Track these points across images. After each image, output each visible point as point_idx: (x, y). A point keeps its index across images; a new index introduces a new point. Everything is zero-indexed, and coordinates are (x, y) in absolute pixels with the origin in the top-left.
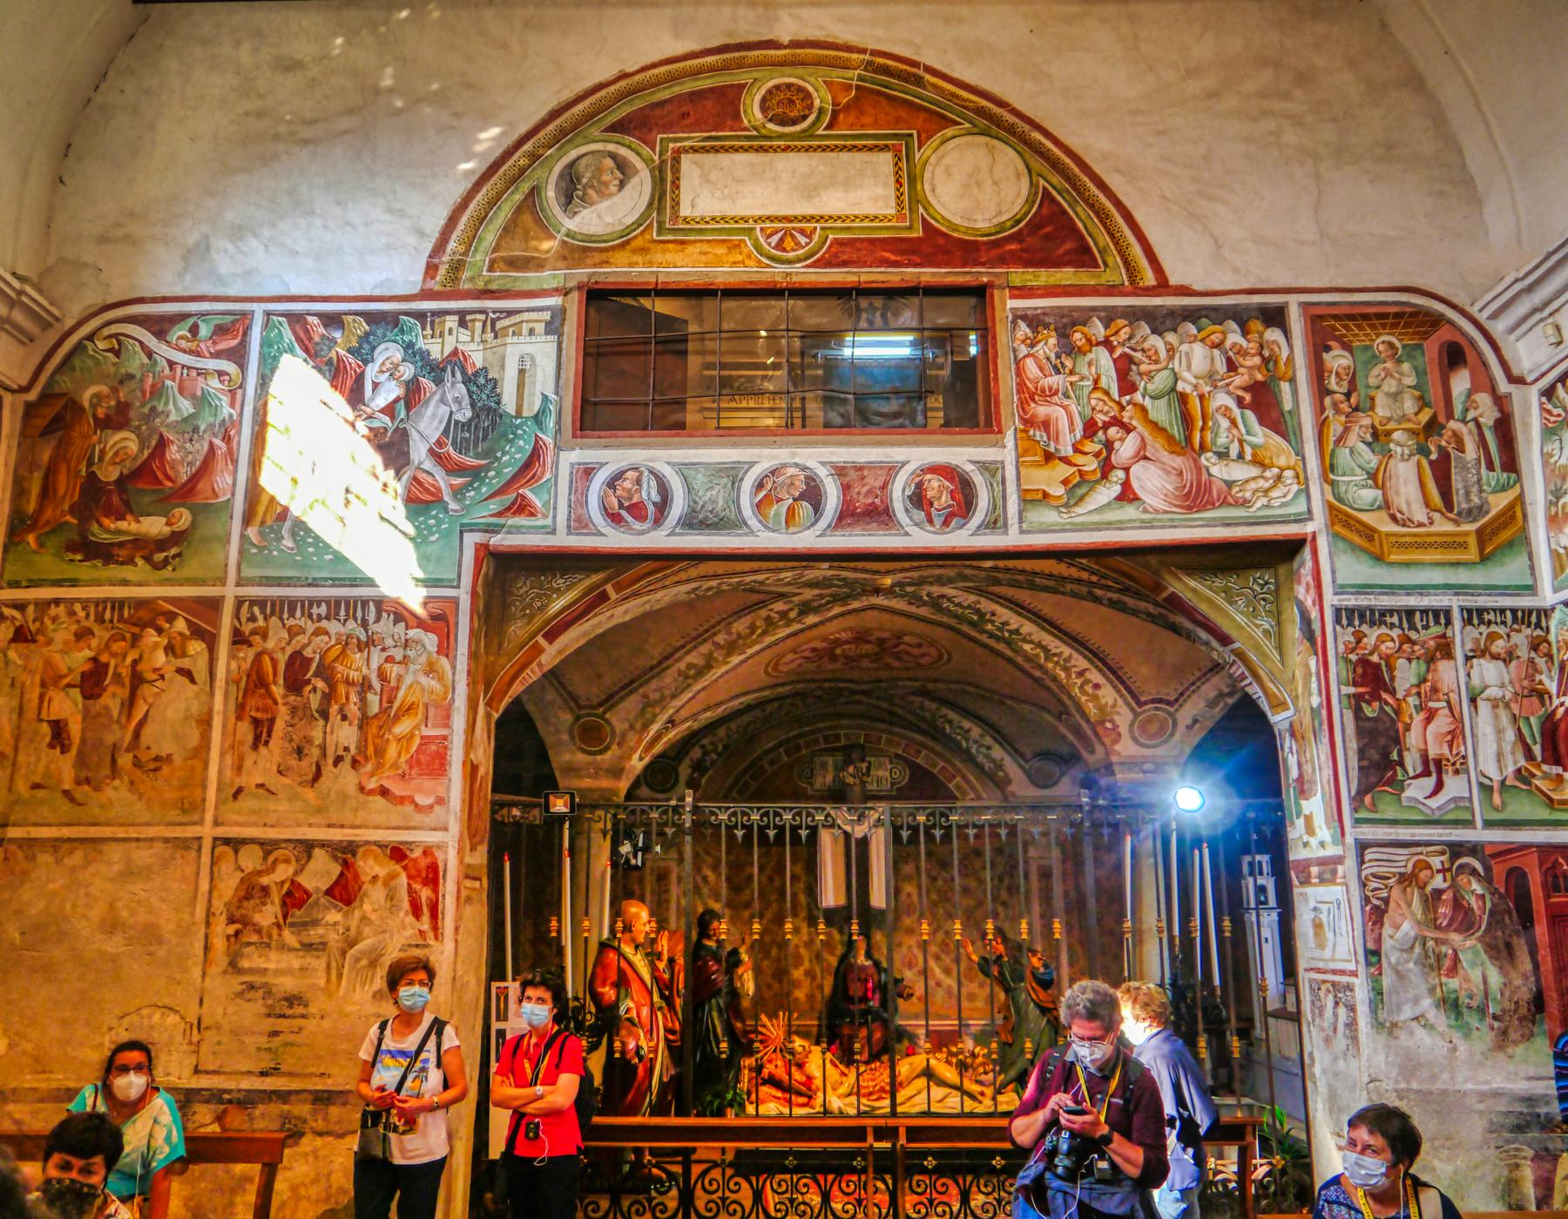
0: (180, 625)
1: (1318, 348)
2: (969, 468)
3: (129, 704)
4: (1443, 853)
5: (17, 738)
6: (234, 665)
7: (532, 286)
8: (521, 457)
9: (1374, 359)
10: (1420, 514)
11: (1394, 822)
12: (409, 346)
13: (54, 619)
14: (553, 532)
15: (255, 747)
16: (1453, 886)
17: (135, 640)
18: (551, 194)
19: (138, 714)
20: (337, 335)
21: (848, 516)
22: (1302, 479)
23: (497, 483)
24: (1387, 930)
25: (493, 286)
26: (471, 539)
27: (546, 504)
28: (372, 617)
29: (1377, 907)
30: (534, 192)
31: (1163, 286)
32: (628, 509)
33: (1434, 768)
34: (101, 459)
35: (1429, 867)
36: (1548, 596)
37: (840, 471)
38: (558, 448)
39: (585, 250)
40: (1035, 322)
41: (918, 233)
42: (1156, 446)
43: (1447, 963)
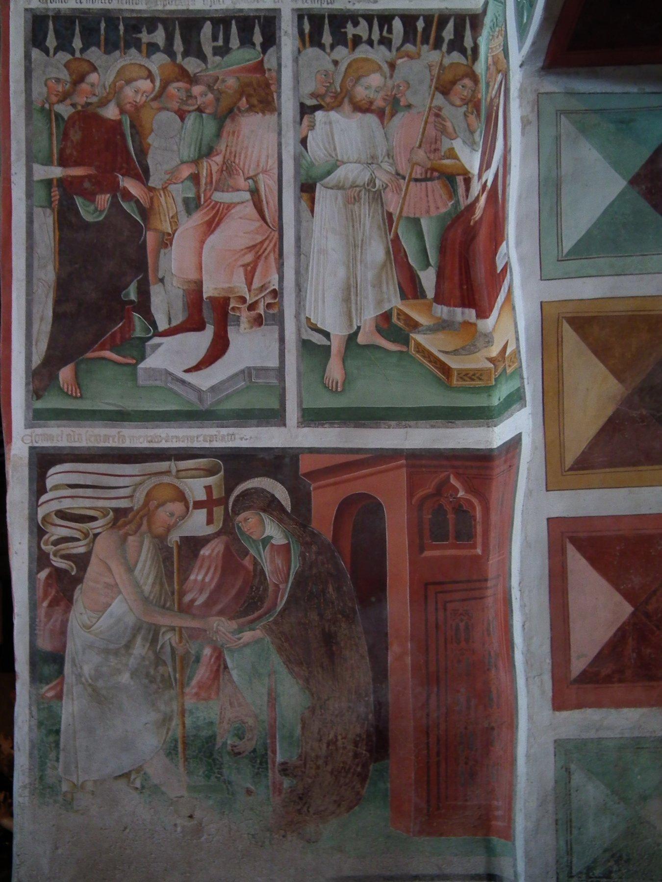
4: (210, 472)
16: (228, 529)
24: (79, 614)
29: (58, 575)
33: (209, 315)
35: (181, 497)
43: (202, 673)
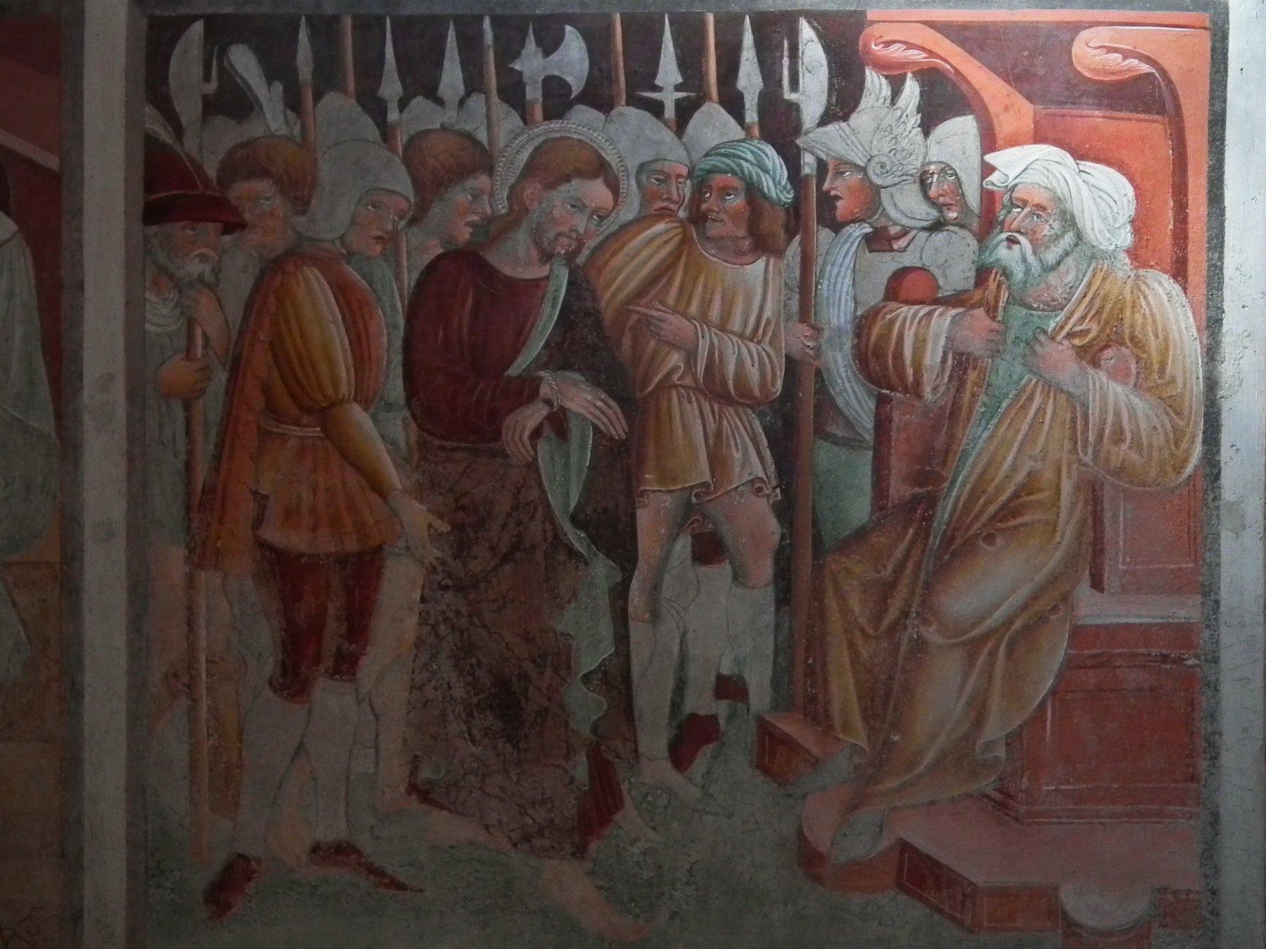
15: (292, 680)
28: (812, 90)
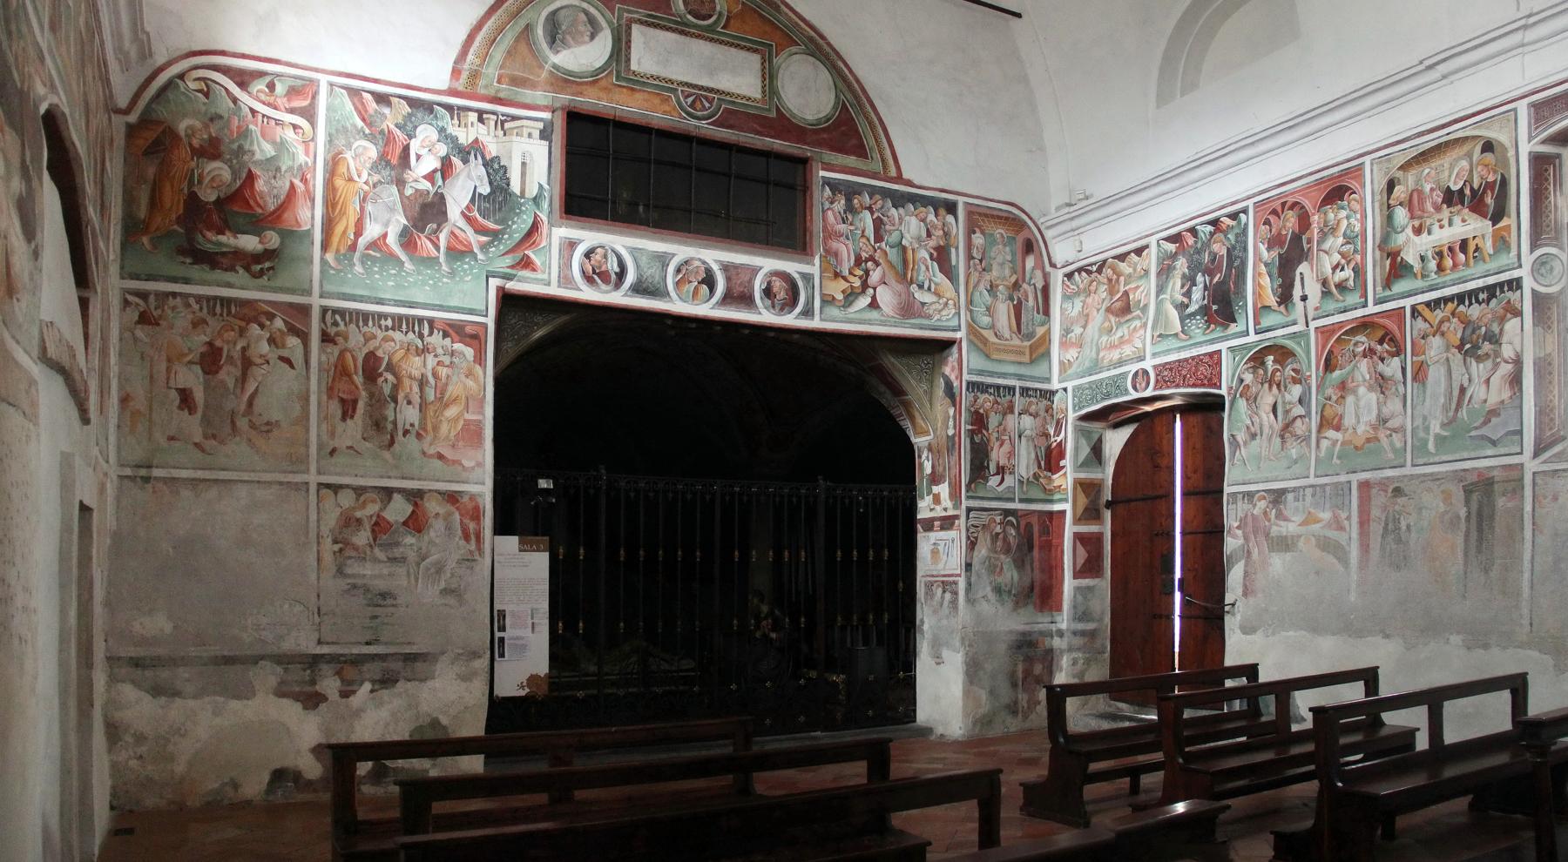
0: (279, 323)
1: (970, 232)
2: (796, 276)
3: (243, 379)
5: (150, 400)
6: (324, 358)
7: (528, 101)
8: (526, 227)
9: (994, 242)
10: (1007, 334)
11: (982, 498)
12: (442, 130)
13: (174, 308)
14: (549, 284)
15: (344, 419)
17: (242, 332)
18: (540, 31)
19: (251, 388)
20: (386, 111)
21: (729, 298)
22: (957, 306)
23: (510, 244)
25: (502, 95)
26: (494, 283)
27: (543, 263)
28: (426, 331)
30: (528, 28)
31: (899, 179)
32: (599, 275)
33: (1001, 470)
34: (200, 182)
36: (1055, 385)
37: (726, 268)
38: (551, 225)
39: (567, 81)
40: (835, 186)
41: (773, 114)
42: (891, 279)
